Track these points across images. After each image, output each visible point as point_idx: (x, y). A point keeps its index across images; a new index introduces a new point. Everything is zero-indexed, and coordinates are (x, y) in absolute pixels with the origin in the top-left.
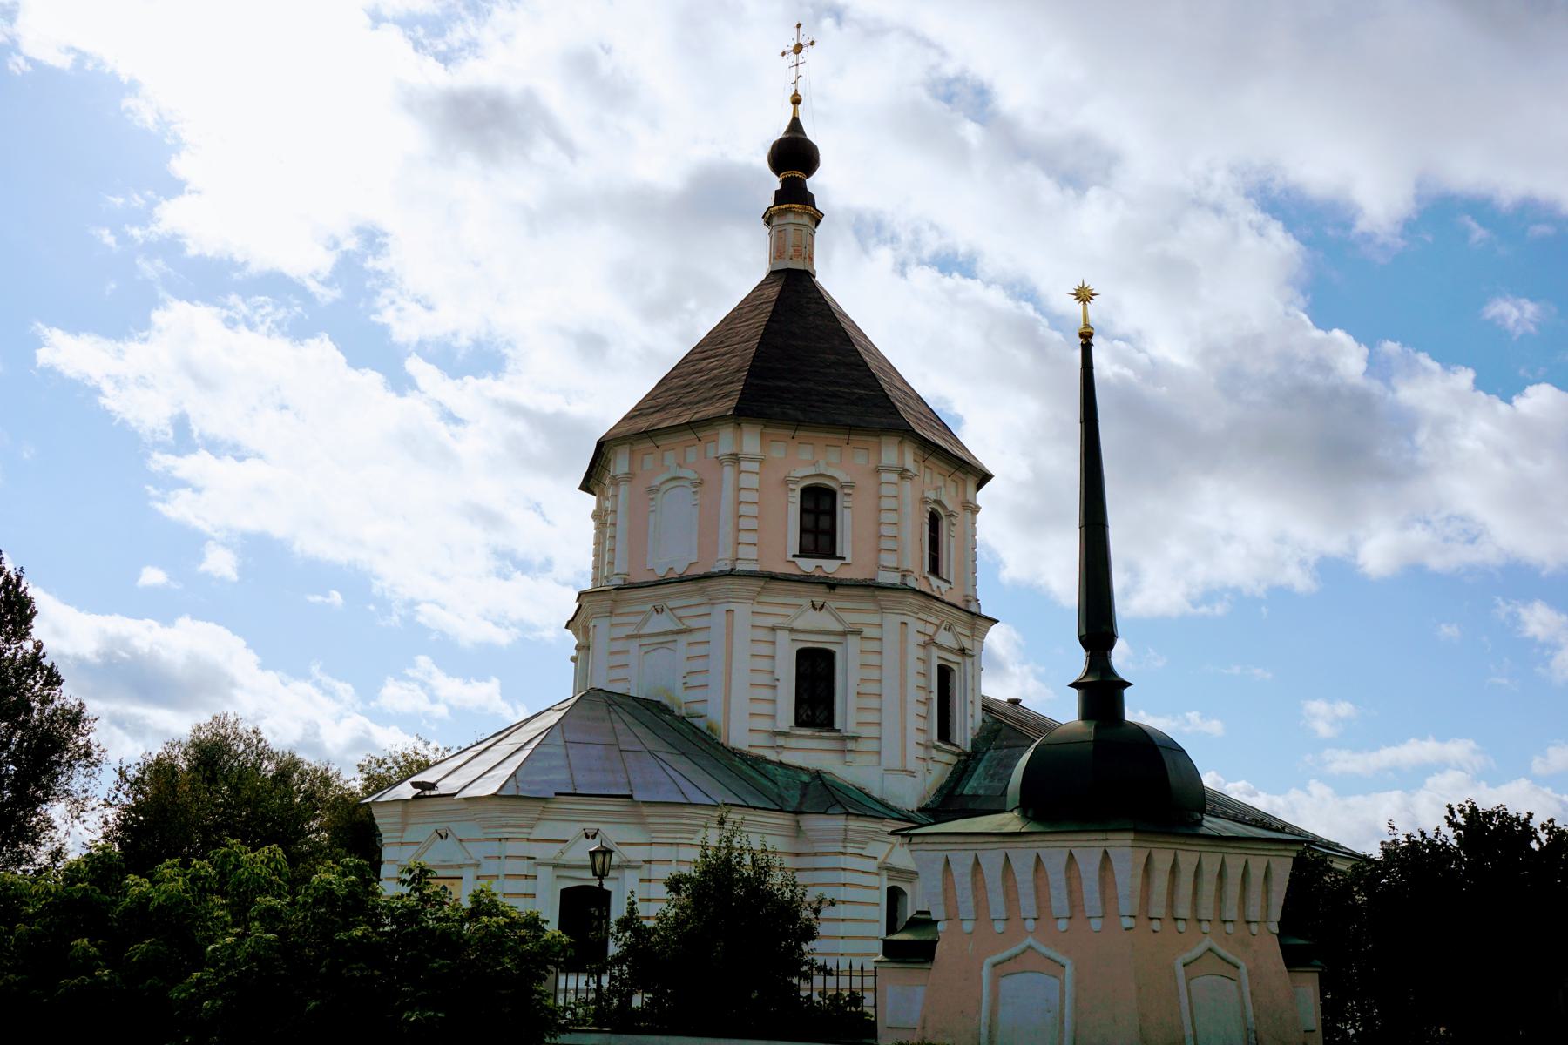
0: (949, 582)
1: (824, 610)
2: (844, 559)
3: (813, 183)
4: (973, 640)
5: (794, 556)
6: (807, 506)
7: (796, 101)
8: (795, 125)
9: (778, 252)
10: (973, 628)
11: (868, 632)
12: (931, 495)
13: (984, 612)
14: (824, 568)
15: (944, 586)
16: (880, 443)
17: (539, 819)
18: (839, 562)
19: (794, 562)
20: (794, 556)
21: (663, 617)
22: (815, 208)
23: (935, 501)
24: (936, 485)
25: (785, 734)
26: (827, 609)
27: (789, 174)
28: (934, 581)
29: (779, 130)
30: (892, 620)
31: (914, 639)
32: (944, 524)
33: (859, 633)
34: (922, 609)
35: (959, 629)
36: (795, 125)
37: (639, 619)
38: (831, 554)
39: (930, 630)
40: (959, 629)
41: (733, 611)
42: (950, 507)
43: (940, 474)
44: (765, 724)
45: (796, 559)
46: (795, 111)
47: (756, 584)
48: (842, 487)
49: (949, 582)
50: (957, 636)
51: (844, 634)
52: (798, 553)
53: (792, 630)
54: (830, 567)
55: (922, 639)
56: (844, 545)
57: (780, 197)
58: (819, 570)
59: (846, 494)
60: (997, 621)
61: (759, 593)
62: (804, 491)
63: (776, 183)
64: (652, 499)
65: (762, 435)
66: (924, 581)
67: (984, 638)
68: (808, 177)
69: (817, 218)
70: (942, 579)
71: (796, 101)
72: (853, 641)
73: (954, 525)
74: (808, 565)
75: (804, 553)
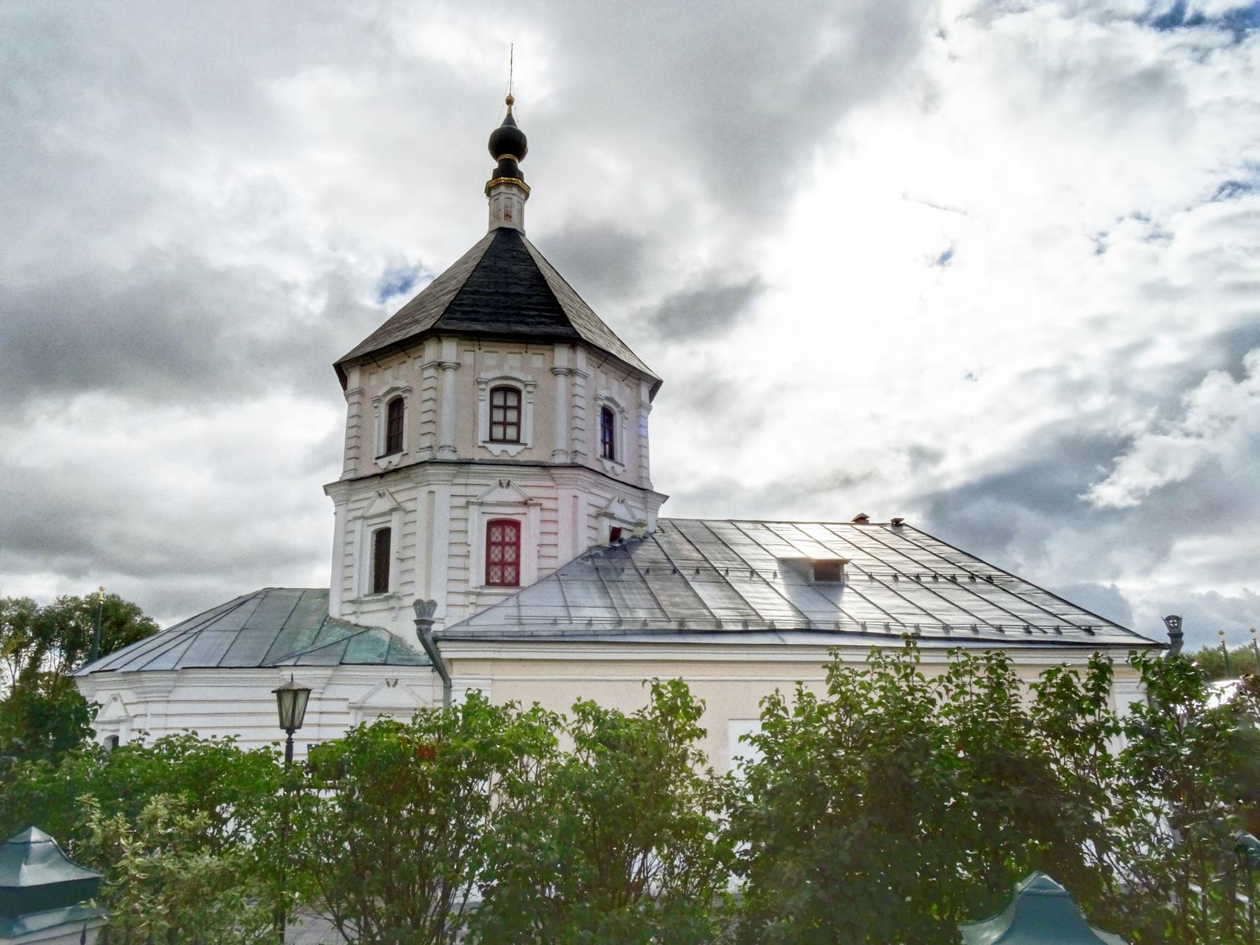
0: (623, 466)
1: (510, 488)
2: (526, 444)
3: (521, 166)
4: (647, 511)
6: (495, 403)
7: (510, 102)
8: (510, 120)
9: (494, 216)
10: (645, 501)
11: (546, 504)
12: (604, 393)
13: (655, 490)
14: (509, 452)
15: (619, 469)
16: (553, 350)
17: (175, 687)
18: (522, 447)
19: (484, 447)
20: (484, 442)
21: (385, 499)
22: (523, 181)
23: (608, 399)
24: (619, 392)
25: (479, 594)
26: (513, 488)
28: (608, 464)
30: (565, 494)
31: (585, 510)
32: (618, 419)
33: (541, 505)
34: (597, 485)
35: (630, 503)
36: (510, 120)
37: (364, 504)
38: (517, 441)
39: (602, 503)
40: (630, 503)
41: (434, 492)
42: (623, 404)
43: (615, 379)
44: (461, 587)
45: (486, 445)
46: (510, 109)
47: (451, 470)
48: (526, 385)
49: (623, 466)
50: (629, 508)
51: (525, 504)
53: (481, 504)
54: (513, 450)
55: (593, 511)
56: (527, 435)
57: (497, 174)
58: (505, 454)
59: (529, 392)
60: (667, 497)
61: (455, 476)
63: (495, 165)
64: (376, 407)
65: (458, 345)
66: (597, 463)
67: (658, 510)
68: (520, 160)
70: (617, 463)
71: (510, 102)
72: (534, 513)
73: (627, 419)
74: (496, 449)
75: (492, 440)
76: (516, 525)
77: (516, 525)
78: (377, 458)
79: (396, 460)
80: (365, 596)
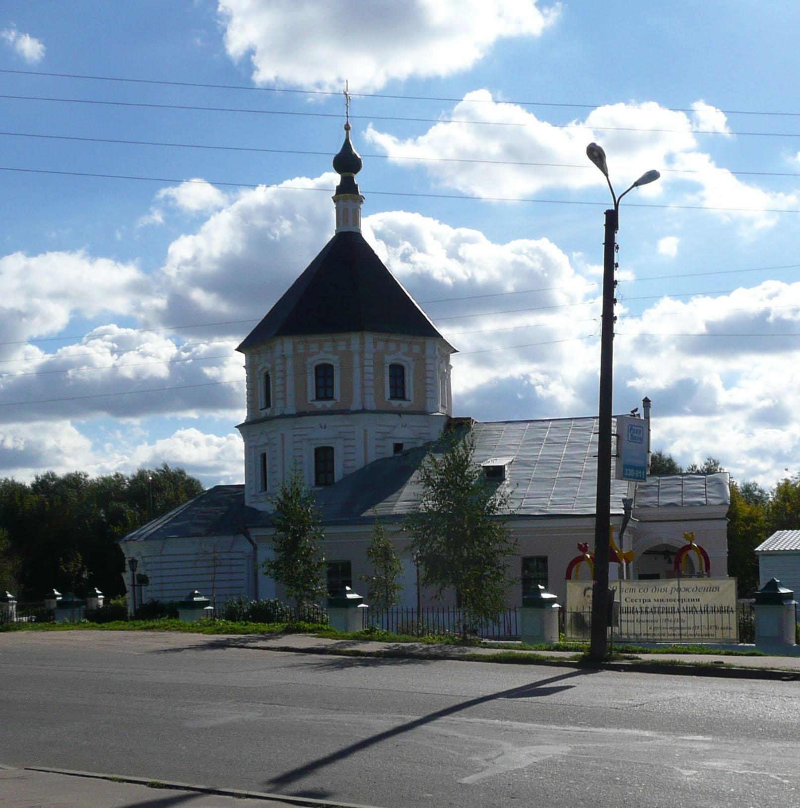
0: (410, 400)
1: (326, 429)
3: (358, 179)
5: (311, 401)
7: (347, 128)
20: (311, 401)
27: (346, 174)
28: (395, 403)
29: (338, 150)
38: (332, 398)
45: (313, 403)
49: (410, 400)
52: (314, 398)
54: (329, 404)
57: (340, 190)
62: (318, 368)
69: (360, 200)
74: (319, 405)
75: (318, 398)
76: (332, 449)
77: (332, 449)
78: (261, 410)
79: (268, 411)
80: (260, 492)
